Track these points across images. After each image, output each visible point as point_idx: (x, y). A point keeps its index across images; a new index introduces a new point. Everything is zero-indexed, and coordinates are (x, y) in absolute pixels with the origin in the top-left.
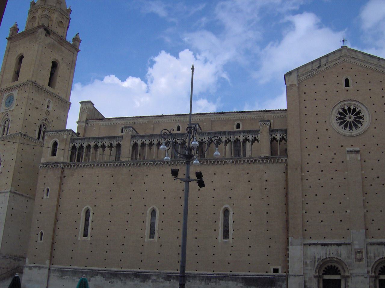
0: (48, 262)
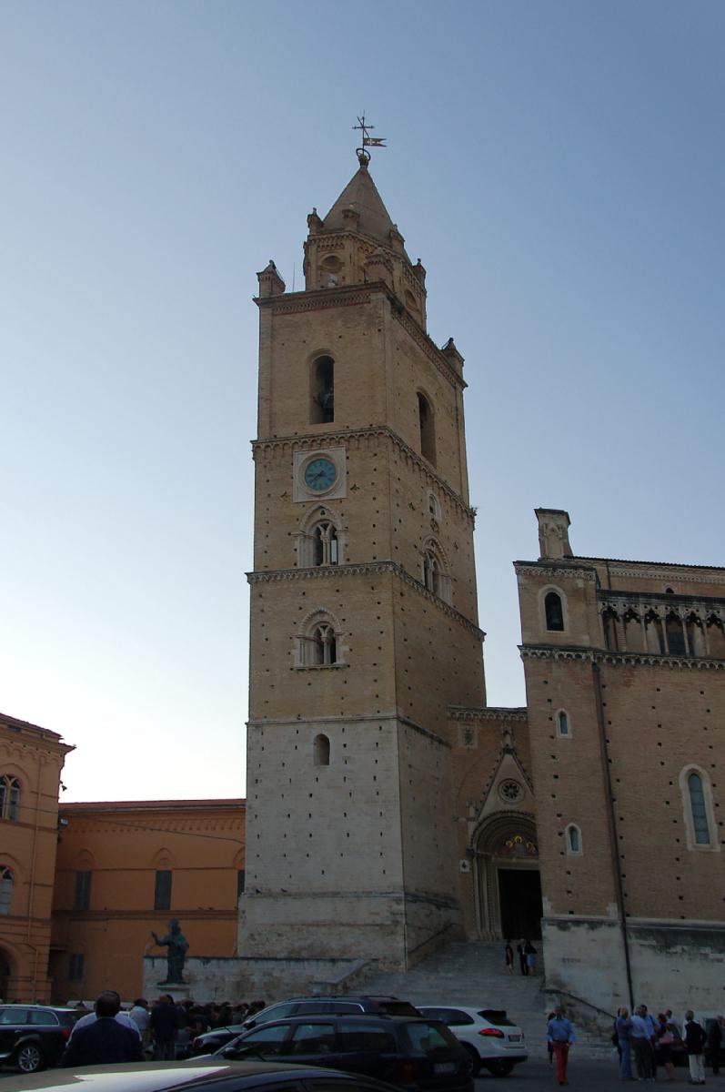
0: (613, 911)
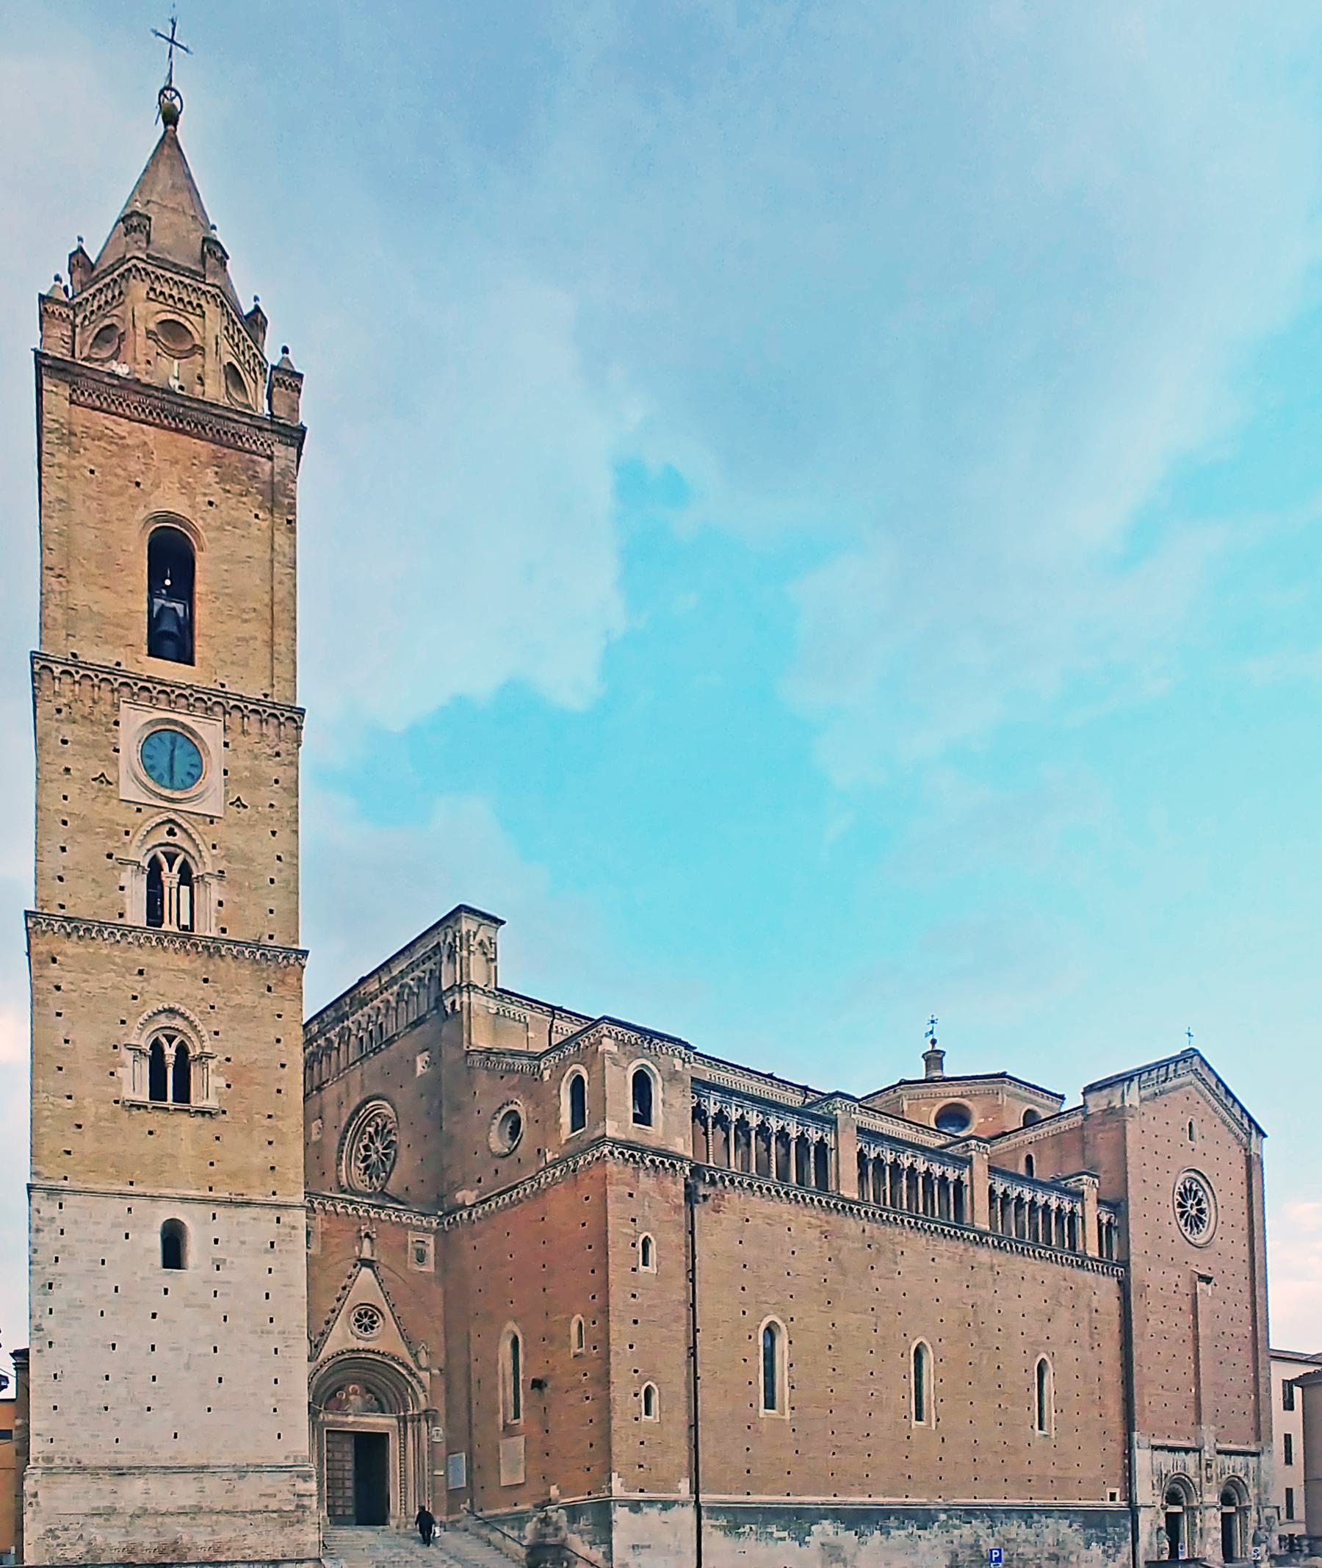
0: (684, 1486)
